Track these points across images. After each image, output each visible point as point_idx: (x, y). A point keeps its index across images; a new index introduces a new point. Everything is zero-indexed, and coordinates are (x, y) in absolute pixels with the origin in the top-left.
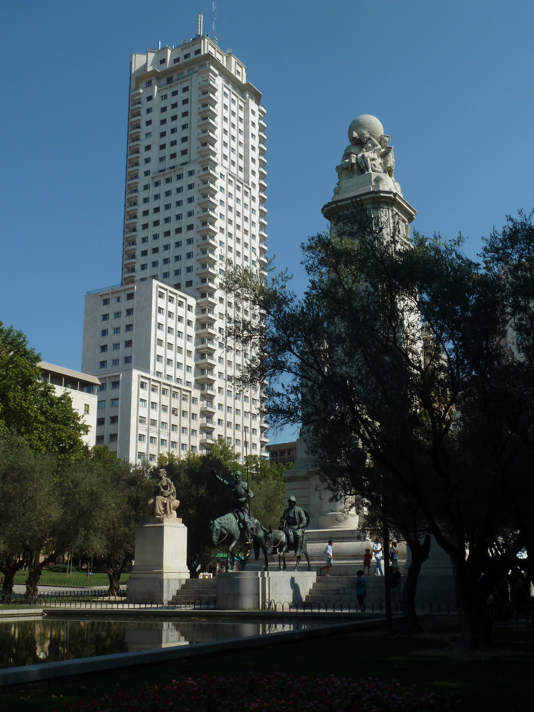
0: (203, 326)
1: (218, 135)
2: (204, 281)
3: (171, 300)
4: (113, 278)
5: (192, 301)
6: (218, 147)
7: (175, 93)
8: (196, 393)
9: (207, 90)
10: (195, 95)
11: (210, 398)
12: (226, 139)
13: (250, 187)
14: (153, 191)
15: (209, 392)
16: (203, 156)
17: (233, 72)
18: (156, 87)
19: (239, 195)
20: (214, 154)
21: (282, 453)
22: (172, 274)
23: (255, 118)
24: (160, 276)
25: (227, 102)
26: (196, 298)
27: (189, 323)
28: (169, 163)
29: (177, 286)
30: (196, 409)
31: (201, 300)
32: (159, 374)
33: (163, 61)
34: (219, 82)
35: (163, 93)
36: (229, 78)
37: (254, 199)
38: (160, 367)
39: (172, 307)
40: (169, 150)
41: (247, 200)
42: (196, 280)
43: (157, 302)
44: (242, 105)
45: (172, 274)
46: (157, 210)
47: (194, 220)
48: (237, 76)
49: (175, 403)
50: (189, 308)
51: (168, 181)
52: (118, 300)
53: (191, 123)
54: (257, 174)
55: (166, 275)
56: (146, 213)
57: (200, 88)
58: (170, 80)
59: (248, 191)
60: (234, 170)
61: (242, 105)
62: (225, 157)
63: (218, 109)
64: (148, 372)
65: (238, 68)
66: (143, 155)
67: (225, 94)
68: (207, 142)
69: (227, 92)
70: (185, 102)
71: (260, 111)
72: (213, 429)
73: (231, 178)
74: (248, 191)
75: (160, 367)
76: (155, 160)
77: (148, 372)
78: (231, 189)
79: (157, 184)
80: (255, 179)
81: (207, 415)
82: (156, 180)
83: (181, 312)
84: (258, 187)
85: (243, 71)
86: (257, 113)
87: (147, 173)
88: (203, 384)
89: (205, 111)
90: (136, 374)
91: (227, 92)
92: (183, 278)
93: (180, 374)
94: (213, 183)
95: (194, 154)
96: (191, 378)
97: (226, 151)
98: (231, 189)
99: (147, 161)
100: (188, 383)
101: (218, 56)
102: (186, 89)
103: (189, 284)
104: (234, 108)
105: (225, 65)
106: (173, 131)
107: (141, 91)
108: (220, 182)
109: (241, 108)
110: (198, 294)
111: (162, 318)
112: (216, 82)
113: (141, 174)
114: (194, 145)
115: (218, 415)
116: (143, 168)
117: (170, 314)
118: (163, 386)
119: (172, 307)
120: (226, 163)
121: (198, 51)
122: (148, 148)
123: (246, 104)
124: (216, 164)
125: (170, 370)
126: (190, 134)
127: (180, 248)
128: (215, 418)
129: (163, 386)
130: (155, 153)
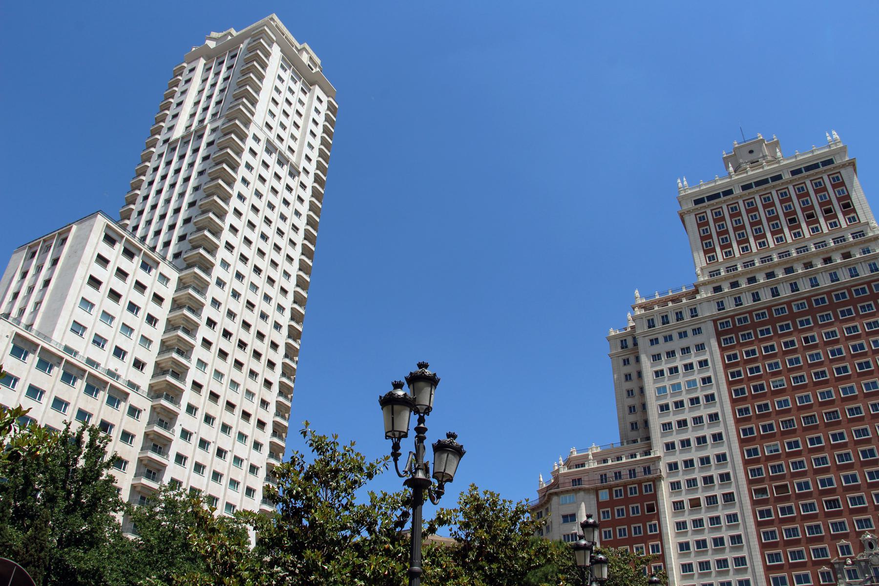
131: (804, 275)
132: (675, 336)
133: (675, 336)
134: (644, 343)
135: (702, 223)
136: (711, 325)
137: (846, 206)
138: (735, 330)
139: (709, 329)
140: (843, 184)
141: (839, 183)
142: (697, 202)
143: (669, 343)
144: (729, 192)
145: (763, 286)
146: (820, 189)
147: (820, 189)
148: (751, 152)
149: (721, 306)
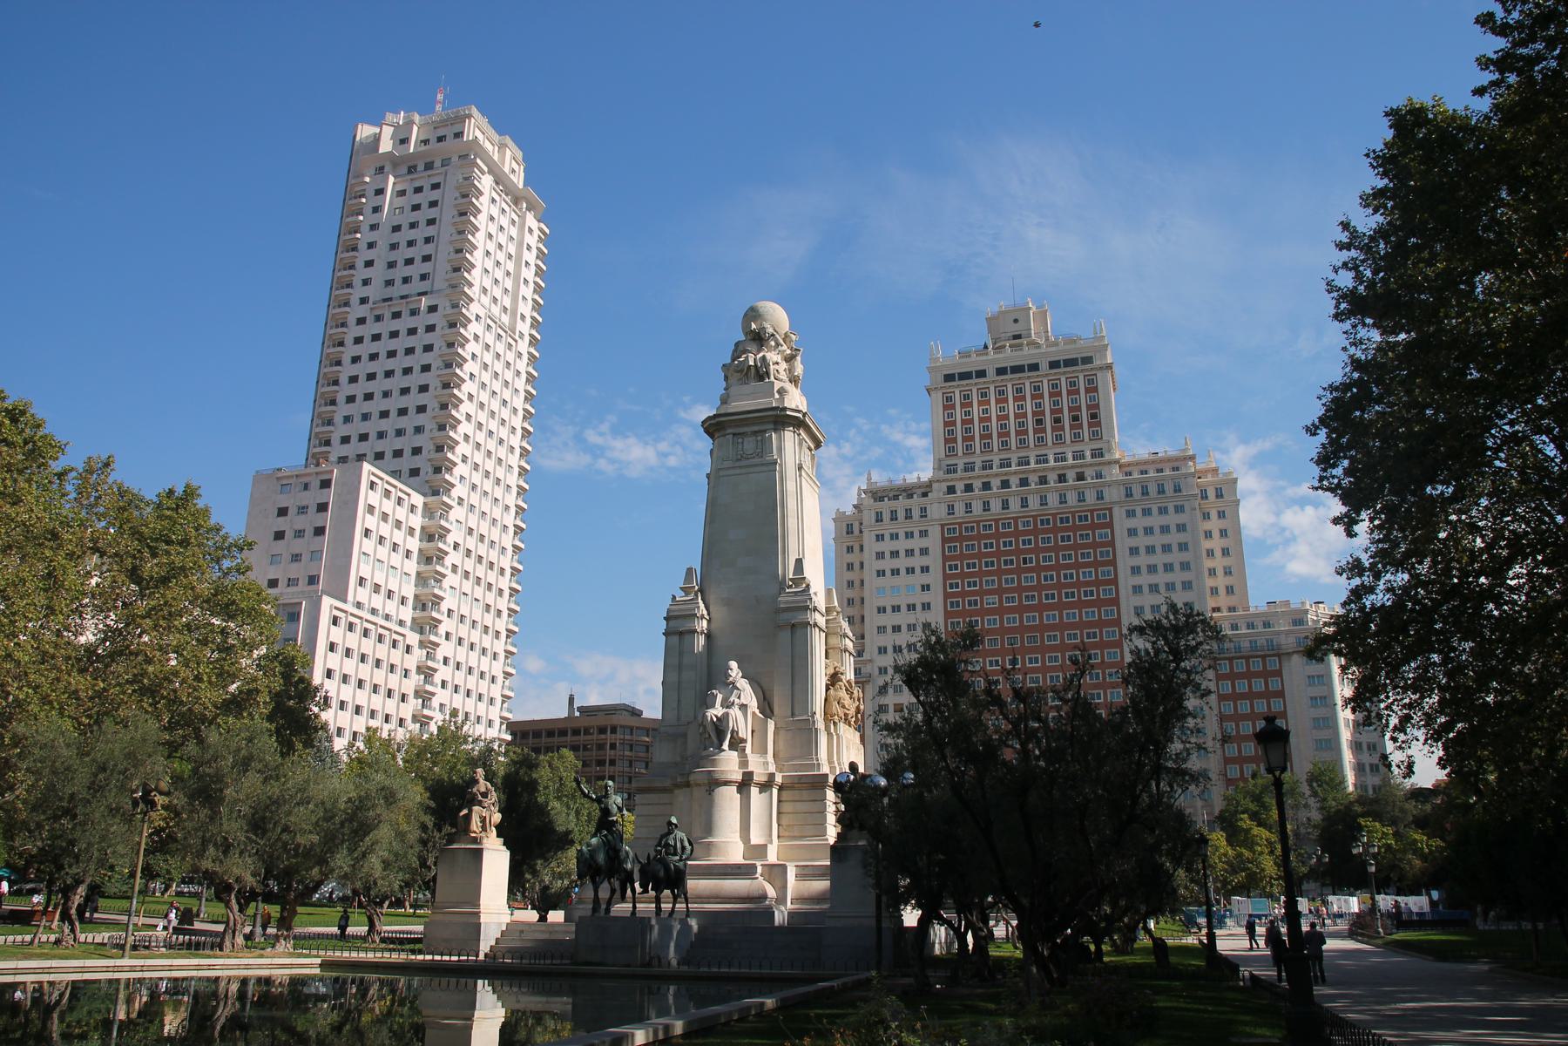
0: (431, 538)
1: (477, 257)
2: (438, 470)
3: (387, 494)
4: (293, 456)
5: (418, 499)
6: (475, 276)
7: (418, 190)
8: (413, 638)
9: (468, 192)
10: (449, 196)
11: (429, 647)
14: (372, 328)
15: (433, 638)
16: (454, 287)
17: (506, 170)
18: (391, 179)
19: (500, 347)
20: (471, 285)
21: (537, 734)
22: (389, 455)
23: (532, 240)
24: (370, 456)
25: (495, 211)
26: (424, 495)
27: (411, 531)
28: (399, 289)
29: (396, 474)
30: (411, 662)
31: (430, 499)
32: (359, 605)
33: (404, 141)
34: (486, 183)
35: (399, 187)
37: (520, 355)
38: (363, 594)
39: (388, 506)
40: (402, 271)
41: (510, 356)
42: (426, 470)
43: (367, 497)
45: (389, 455)
46: (373, 357)
47: (430, 378)
49: (382, 651)
50: (413, 508)
51: (396, 315)
52: (306, 487)
54: (529, 320)
55: (379, 456)
56: (356, 360)
57: (457, 188)
58: (412, 170)
60: (496, 310)
62: (485, 291)
63: (481, 221)
64: (345, 601)
65: (515, 165)
66: (361, 273)
67: (493, 201)
68: (459, 267)
69: (497, 198)
70: (433, 204)
71: (541, 230)
72: (433, 694)
73: (491, 323)
75: (363, 594)
76: (378, 282)
77: (345, 601)
78: (490, 338)
79: (378, 318)
80: (524, 327)
81: (427, 672)
82: (378, 312)
83: (401, 513)
84: (527, 338)
85: (520, 171)
86: (536, 232)
87: (363, 301)
88: (425, 626)
89: (463, 223)
90: (327, 602)
91: (497, 198)
92: (407, 462)
93: (391, 607)
94: (465, 326)
95: (439, 283)
96: (407, 614)
97: (488, 283)
98: (490, 338)
99: (366, 282)
100: (401, 623)
102: (435, 186)
103: (415, 472)
104: (505, 222)
105: (496, 158)
106: (411, 244)
107: (367, 179)
108: (474, 328)
109: (513, 222)
110: (427, 490)
111: (371, 522)
113: (355, 300)
114: (441, 266)
115: (444, 673)
116: (358, 292)
117: (385, 517)
118: (381, 631)
119: (388, 506)
120: (486, 300)
121: (459, 135)
122: (369, 264)
123: (522, 218)
124: (472, 300)
125: (377, 601)
127: (405, 418)
128: (438, 678)
129: (381, 631)
130: (378, 273)
131: (1037, 492)
132: (902, 535)
133: (902, 535)
134: (868, 538)
135: (948, 405)
136: (938, 529)
137: (1094, 416)
138: (961, 539)
139: (935, 533)
140: (1095, 390)
141: (1092, 389)
142: (949, 378)
143: (895, 542)
144: (981, 374)
145: (996, 496)
146: (1073, 391)
147: (1073, 391)
148: (1016, 321)
149: (951, 508)
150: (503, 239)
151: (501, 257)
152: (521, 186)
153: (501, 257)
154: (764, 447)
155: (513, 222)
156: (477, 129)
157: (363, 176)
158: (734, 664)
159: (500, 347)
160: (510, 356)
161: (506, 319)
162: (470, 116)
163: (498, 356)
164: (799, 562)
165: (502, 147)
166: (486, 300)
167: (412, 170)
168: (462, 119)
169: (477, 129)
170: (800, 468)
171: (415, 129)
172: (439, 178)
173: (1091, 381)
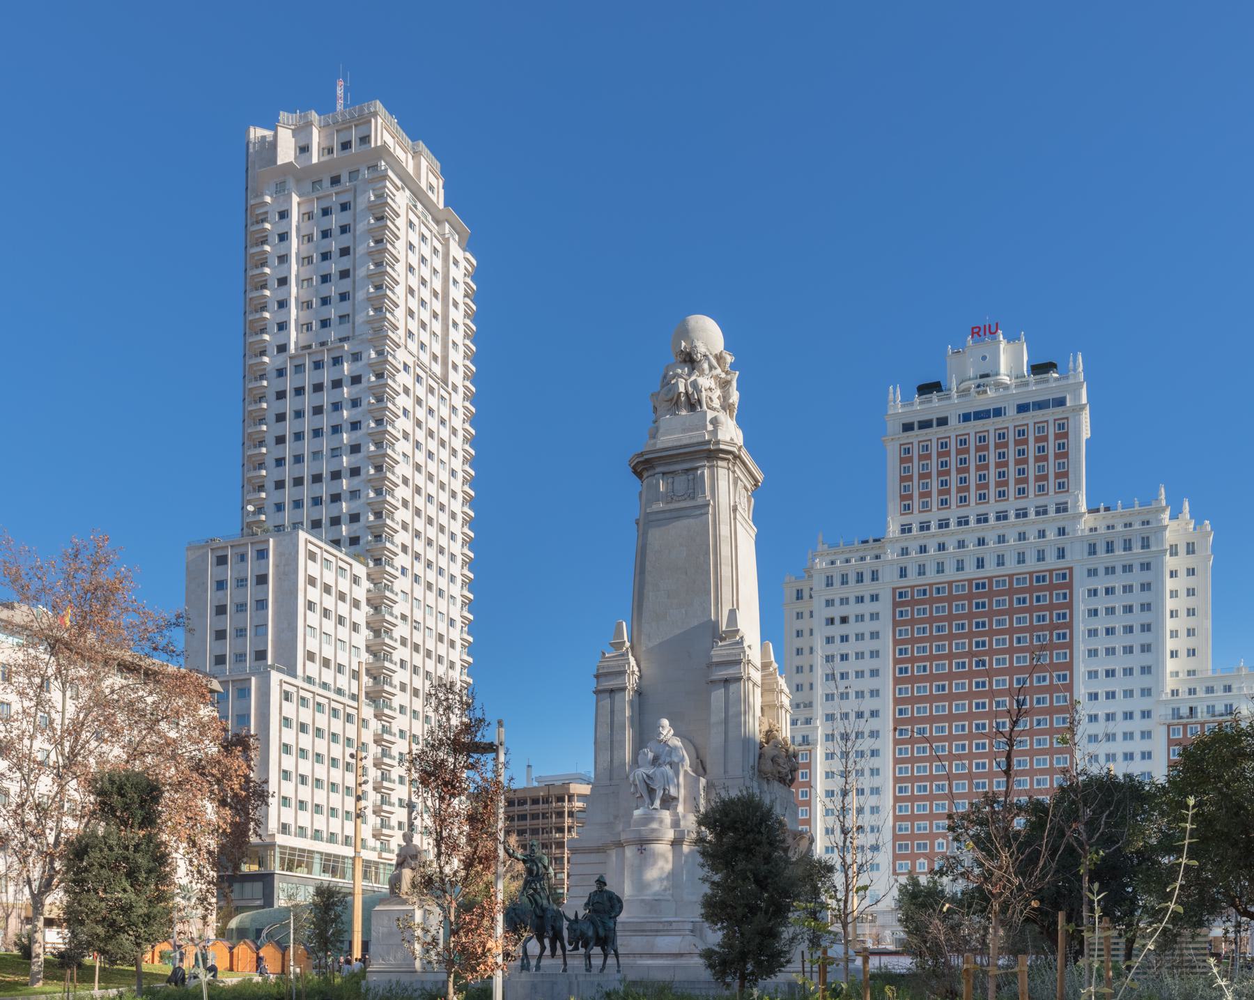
9: (381, 213)
12: (413, 303)
13: (450, 389)
17: (424, 185)
23: (457, 273)
36: (418, 195)
37: (454, 409)
41: (445, 412)
44: (439, 247)
48: (430, 193)
53: (354, 269)
59: (446, 396)
60: (425, 358)
61: (439, 247)
74: (446, 396)
78: (421, 391)
98: (421, 391)
101: (399, 153)
105: (410, 170)
109: (435, 251)
112: (397, 199)
121: (365, 139)
126: (354, 289)
150: (426, 272)
151: (425, 294)
152: (441, 206)
153: (425, 294)
154: (695, 487)
155: (435, 251)
156: (385, 132)
157: (262, 195)
158: (665, 722)
159: (433, 402)
160: (445, 412)
161: (437, 369)
162: (375, 114)
163: (431, 411)
164: (733, 613)
165: (416, 155)
166: (413, 346)
167: (317, 183)
168: (364, 121)
169: (385, 132)
170: (735, 509)
171: (315, 132)
172: (348, 201)
173: (1061, 426)
